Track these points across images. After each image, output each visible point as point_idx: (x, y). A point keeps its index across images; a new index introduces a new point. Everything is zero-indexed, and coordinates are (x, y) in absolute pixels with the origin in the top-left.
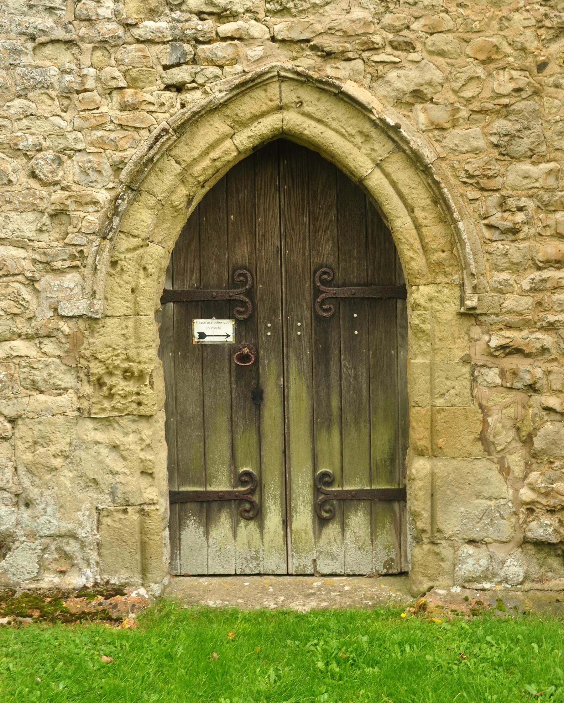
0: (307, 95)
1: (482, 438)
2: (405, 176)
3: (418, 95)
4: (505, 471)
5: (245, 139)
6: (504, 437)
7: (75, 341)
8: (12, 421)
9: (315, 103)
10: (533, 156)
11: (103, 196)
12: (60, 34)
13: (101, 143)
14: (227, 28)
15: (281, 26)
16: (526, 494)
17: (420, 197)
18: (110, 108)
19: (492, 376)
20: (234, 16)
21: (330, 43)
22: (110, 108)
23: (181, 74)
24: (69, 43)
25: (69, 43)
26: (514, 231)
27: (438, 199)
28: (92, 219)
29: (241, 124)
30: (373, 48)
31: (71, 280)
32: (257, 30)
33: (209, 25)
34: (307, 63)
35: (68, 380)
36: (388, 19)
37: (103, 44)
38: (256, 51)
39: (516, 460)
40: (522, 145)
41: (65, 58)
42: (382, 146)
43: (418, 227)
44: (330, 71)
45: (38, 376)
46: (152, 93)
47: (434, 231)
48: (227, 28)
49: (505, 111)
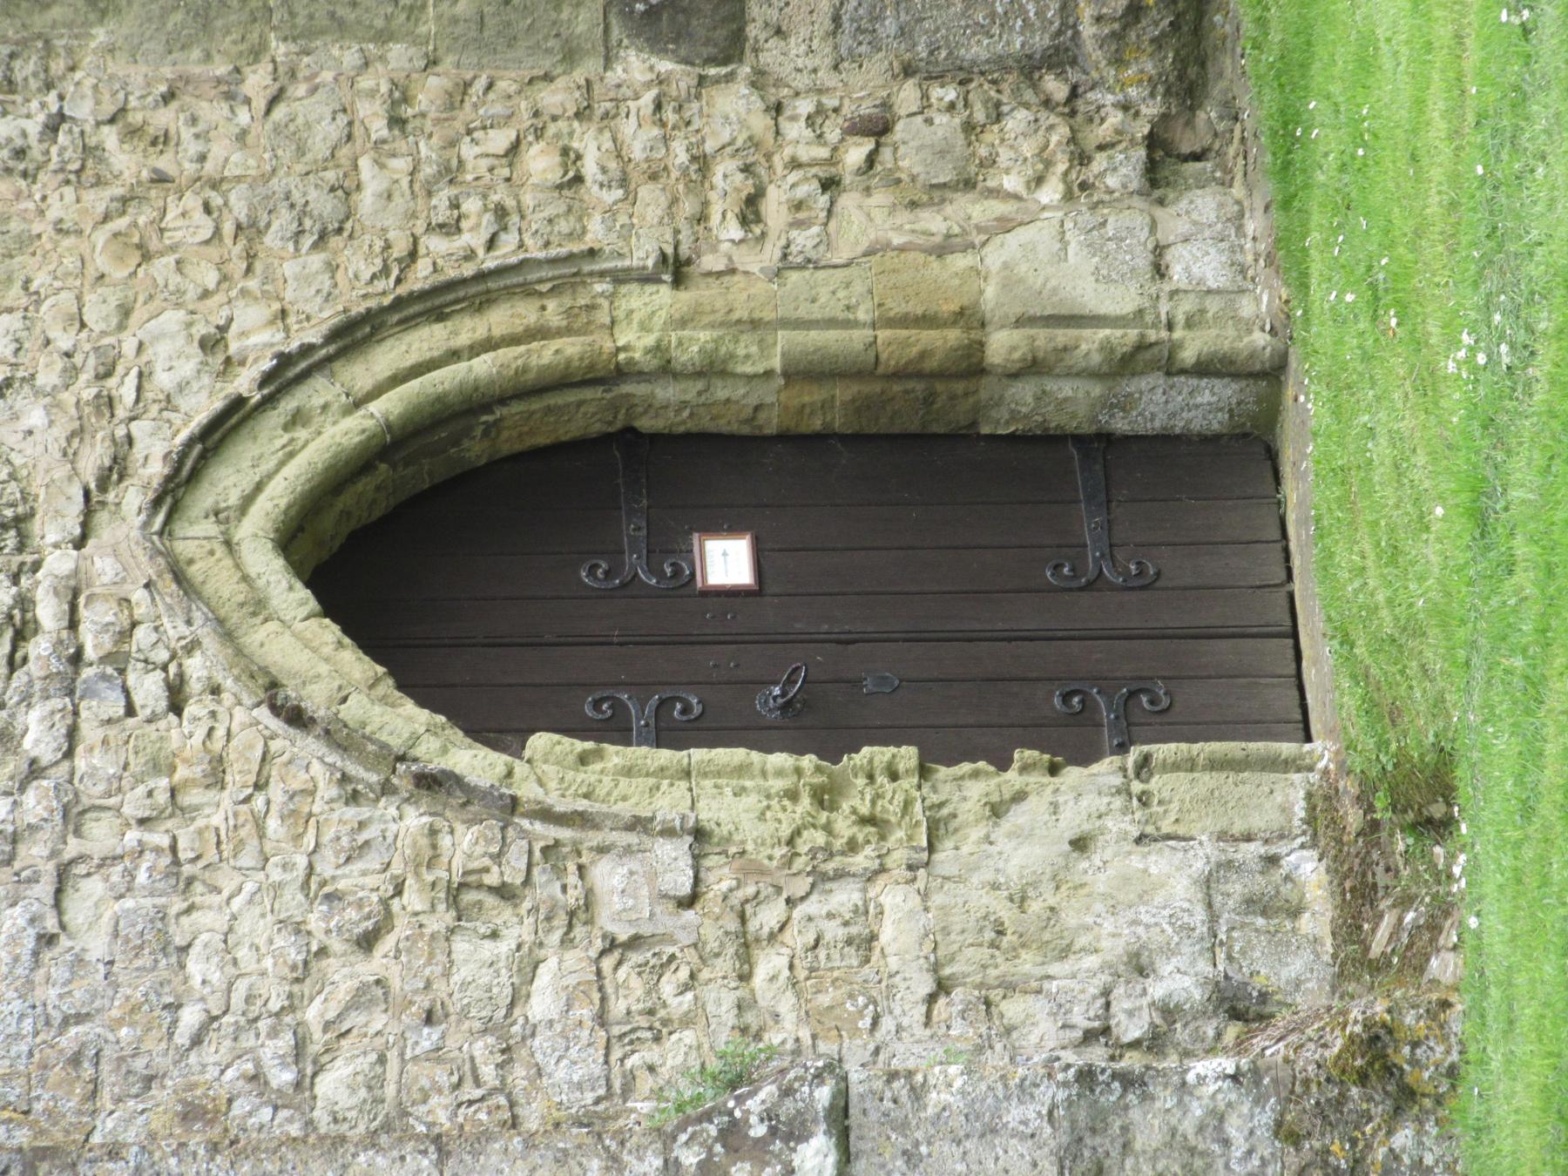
0: (204, 497)
1: (941, 250)
2: (387, 357)
3: (210, 344)
4: (1006, 225)
5: (292, 598)
6: (934, 223)
7: (749, 869)
8: (942, 987)
9: (227, 480)
10: (346, 190)
11: (414, 820)
12: (44, 889)
13: (298, 819)
14: (48, 612)
15: (52, 529)
16: (1051, 192)
17: (426, 340)
18: (217, 809)
19: (804, 240)
20: (24, 602)
21: (94, 457)
22: (217, 809)
23: (149, 689)
24: (63, 876)
25: (63, 876)
26: (501, 212)
27: (437, 303)
28: (465, 844)
29: (258, 606)
30: (108, 403)
31: (609, 876)
32: (59, 563)
33: (39, 648)
34: (133, 498)
35: (845, 897)
36: (48, 377)
37: (73, 816)
38: (103, 568)
39: (980, 210)
40: (325, 206)
41: (89, 892)
42: (318, 392)
43: (488, 345)
44: (151, 466)
45: (834, 931)
46: (184, 737)
47: (500, 319)
48: (48, 612)
49: (250, 230)
